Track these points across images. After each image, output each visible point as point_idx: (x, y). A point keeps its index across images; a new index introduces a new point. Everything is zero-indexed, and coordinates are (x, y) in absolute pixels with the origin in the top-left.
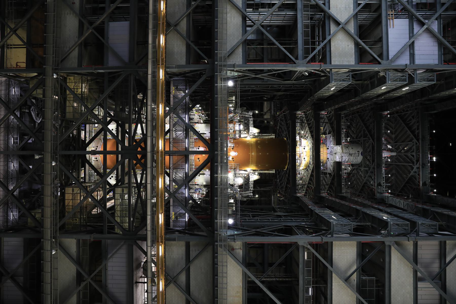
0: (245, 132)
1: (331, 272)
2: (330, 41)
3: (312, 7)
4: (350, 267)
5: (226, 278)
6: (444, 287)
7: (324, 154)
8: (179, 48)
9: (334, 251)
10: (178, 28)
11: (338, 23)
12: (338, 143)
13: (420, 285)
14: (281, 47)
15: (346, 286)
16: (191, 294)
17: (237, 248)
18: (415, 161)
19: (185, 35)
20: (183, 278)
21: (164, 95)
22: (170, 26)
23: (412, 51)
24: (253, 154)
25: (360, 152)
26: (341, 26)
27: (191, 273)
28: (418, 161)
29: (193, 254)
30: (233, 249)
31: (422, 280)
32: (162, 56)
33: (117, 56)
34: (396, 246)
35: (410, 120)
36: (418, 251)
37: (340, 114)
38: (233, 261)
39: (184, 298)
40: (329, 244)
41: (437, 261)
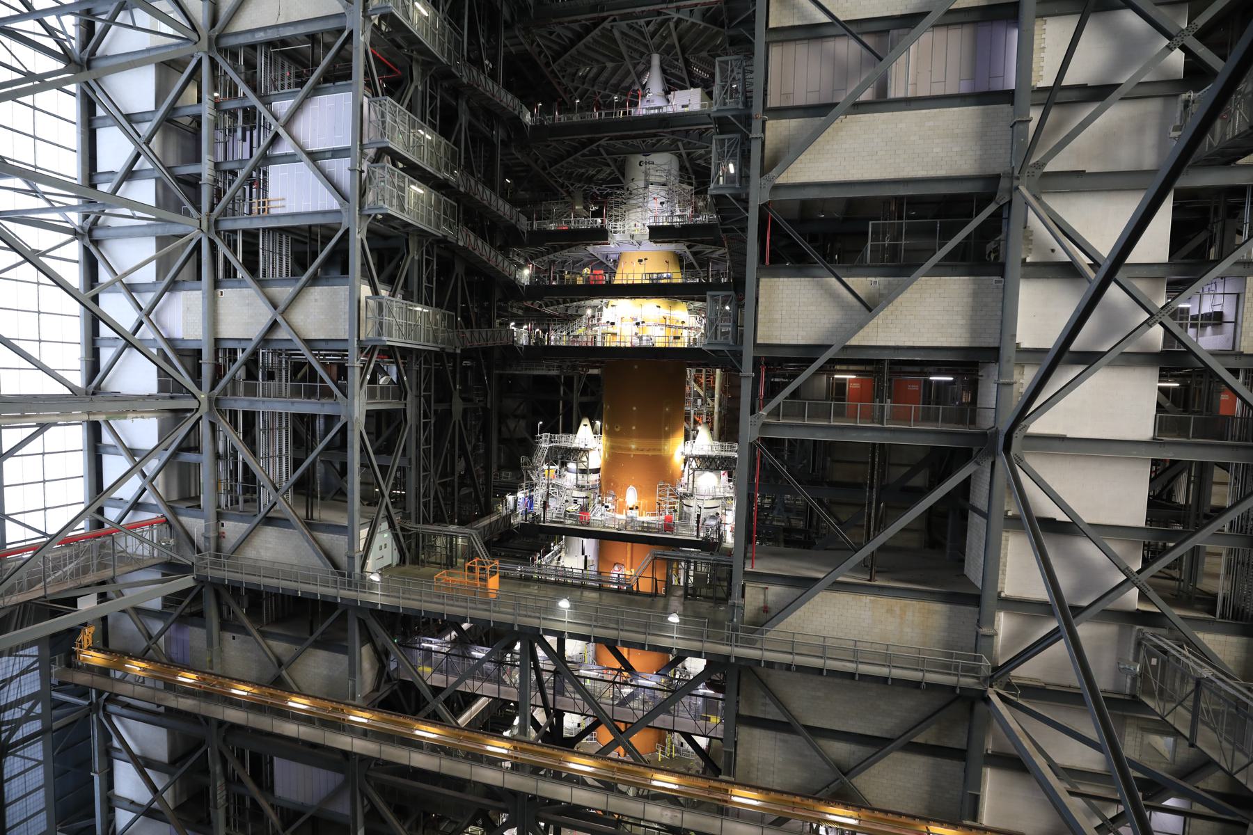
0: (584, 459)
1: (846, 348)
2: (307, 342)
3: (251, 375)
4: (834, 296)
5: (827, 651)
6: (910, 21)
7: (630, 273)
8: (318, 665)
9: (784, 342)
10: (285, 659)
11: (274, 325)
12: (601, 235)
13: (895, 92)
14: (320, 447)
15: (890, 307)
16: (888, 736)
17: (762, 597)
18: (660, 18)
19: (298, 648)
20: (839, 750)
21: (401, 719)
22: (278, 681)
23: (328, 155)
24: (633, 447)
25: (643, 158)
26: (279, 319)
27: (828, 727)
28: (659, 13)
29: (773, 713)
30: (765, 609)
31: (883, 88)
32: (326, 709)
33: (334, 795)
34: (773, 173)
35: (559, 36)
36: (797, 103)
37: (531, 233)
38: (798, 613)
39: (897, 755)
40: (763, 354)
41: (830, 45)
